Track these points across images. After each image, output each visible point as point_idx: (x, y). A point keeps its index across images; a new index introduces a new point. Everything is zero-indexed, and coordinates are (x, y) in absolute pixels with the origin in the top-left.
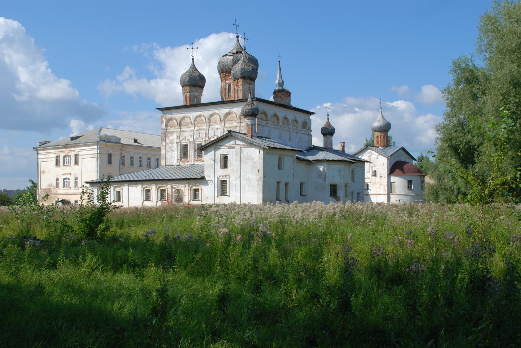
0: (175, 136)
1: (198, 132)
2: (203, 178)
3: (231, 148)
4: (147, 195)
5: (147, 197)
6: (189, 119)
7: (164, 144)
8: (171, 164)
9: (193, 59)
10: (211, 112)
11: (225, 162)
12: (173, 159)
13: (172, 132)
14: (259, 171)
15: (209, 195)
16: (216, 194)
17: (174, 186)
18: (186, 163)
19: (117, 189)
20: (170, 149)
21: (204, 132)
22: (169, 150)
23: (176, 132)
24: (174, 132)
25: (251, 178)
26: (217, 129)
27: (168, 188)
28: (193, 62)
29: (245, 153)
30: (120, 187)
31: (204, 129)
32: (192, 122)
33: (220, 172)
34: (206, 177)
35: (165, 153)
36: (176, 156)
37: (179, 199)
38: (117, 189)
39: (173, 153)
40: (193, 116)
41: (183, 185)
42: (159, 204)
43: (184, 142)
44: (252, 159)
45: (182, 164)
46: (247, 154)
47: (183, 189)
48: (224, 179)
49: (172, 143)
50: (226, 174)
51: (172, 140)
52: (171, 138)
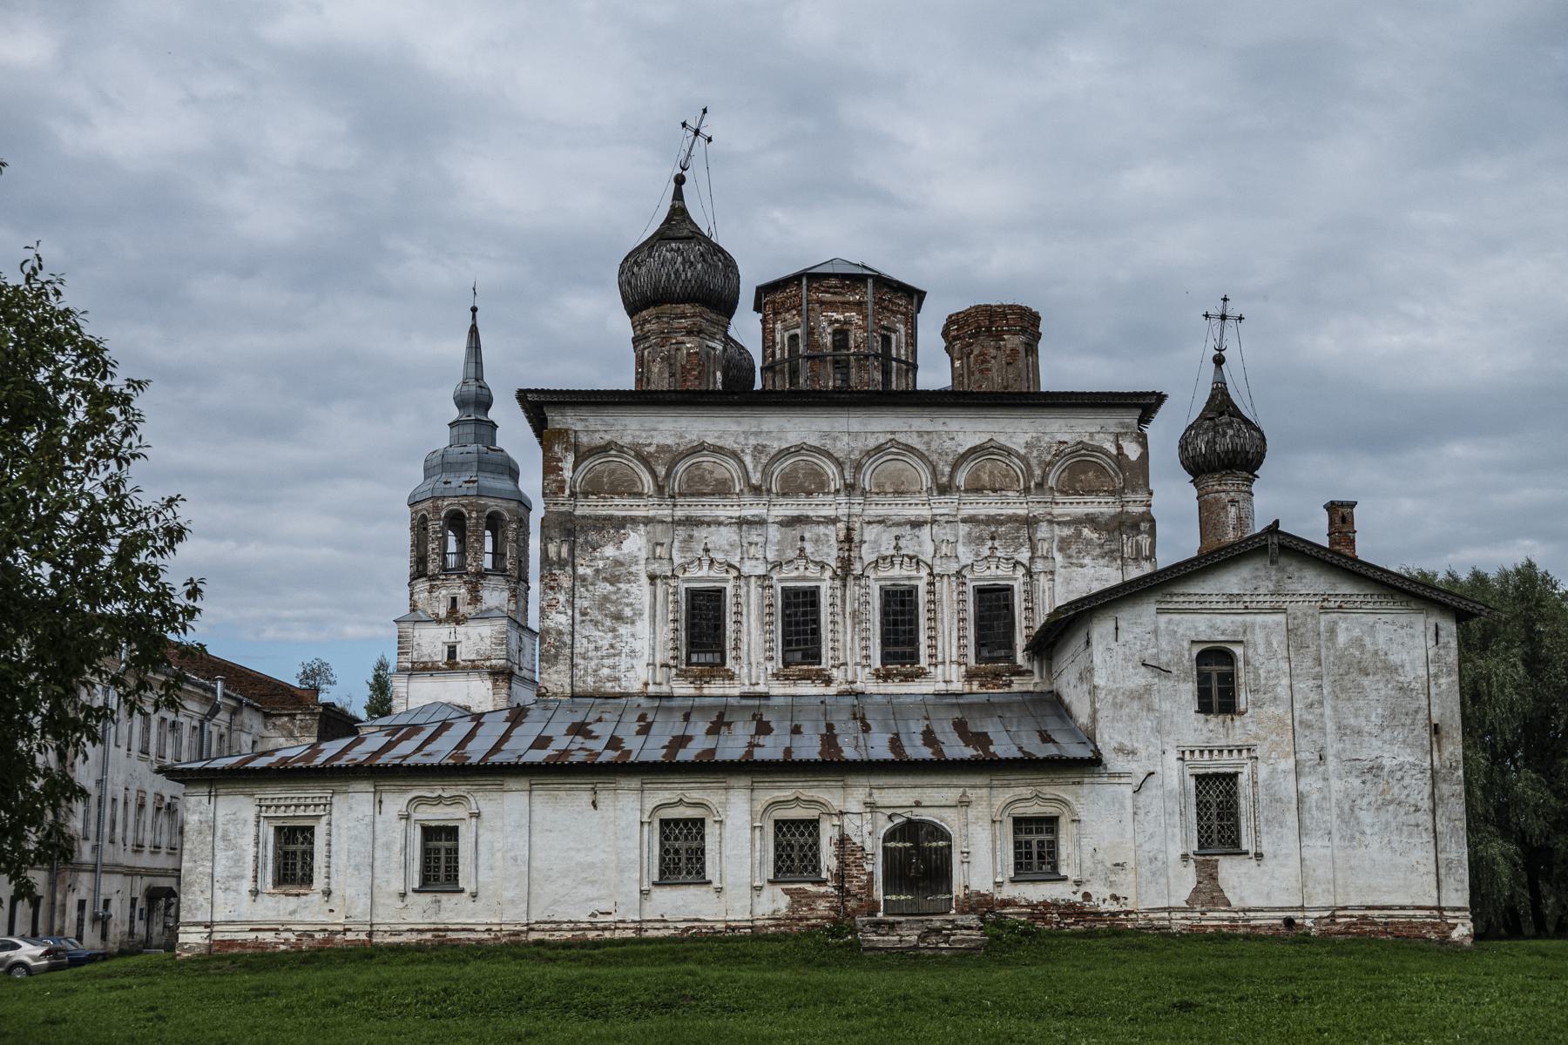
0: (635, 543)
1: (796, 532)
2: (1093, 764)
3: (1260, 611)
4: (681, 852)
6: (732, 464)
7: (566, 582)
9: (680, 180)
11: (1217, 681)
12: (624, 662)
13: (621, 523)
14: (1436, 730)
15: (1127, 852)
16: (1176, 850)
17: (882, 797)
18: (715, 688)
19: (436, 815)
20: (601, 607)
21: (833, 533)
22: (595, 614)
23: (648, 521)
24: (634, 521)
25: (1388, 763)
26: (916, 524)
28: (678, 195)
29: (1342, 639)
30: (456, 800)
31: (833, 521)
32: (756, 479)
33: (1195, 728)
34: (1107, 755)
35: (567, 629)
36: (642, 646)
39: (623, 630)
42: (775, 902)
43: (702, 576)
44: (1392, 669)
45: (683, 688)
47: (950, 820)
48: (1223, 764)
49: (613, 580)
50: (1237, 738)
51: (618, 563)
52: (609, 551)
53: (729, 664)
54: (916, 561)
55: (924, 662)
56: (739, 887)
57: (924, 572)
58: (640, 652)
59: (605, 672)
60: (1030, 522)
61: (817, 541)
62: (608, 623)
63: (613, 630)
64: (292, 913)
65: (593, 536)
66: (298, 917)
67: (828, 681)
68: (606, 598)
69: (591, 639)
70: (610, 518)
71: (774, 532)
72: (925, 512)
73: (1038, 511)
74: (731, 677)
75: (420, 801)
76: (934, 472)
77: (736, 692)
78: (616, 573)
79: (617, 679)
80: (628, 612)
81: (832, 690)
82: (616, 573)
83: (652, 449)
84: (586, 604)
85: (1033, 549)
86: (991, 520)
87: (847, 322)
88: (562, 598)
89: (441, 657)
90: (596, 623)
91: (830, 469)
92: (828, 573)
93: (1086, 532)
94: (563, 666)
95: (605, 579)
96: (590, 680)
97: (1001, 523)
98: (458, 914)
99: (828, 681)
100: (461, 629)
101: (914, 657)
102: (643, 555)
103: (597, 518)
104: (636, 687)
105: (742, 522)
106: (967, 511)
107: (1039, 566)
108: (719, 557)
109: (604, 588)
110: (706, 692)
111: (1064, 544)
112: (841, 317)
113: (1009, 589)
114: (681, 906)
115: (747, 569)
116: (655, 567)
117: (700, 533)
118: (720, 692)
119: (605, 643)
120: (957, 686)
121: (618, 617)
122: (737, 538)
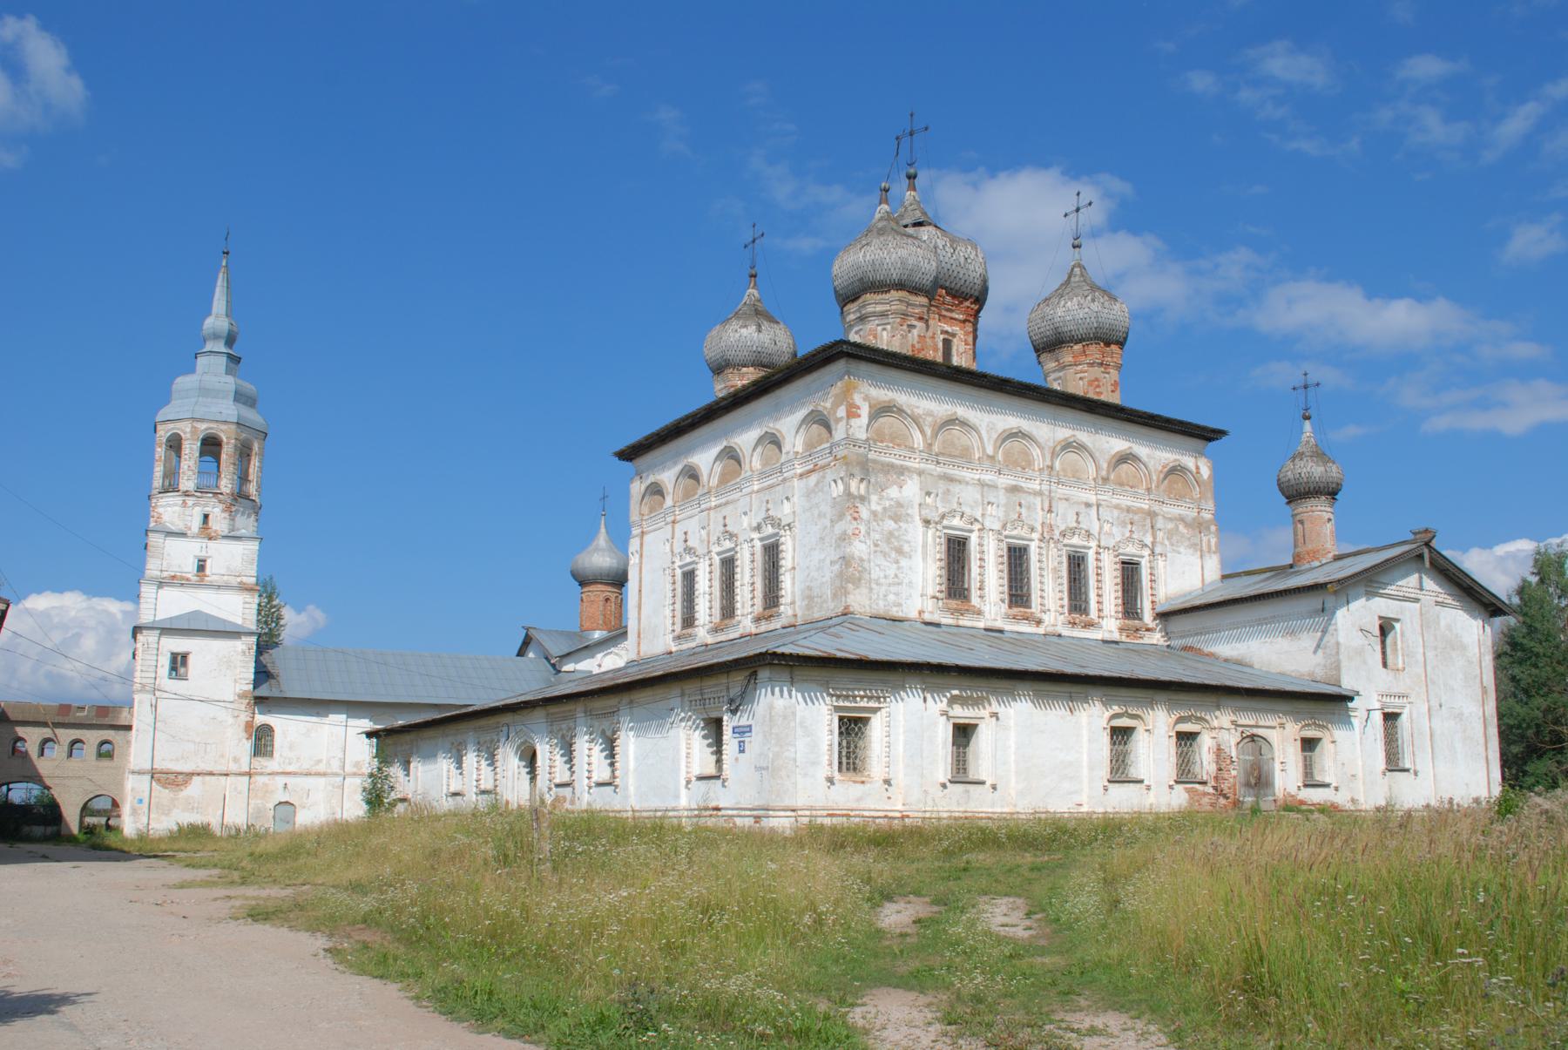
0: (911, 490)
1: (1016, 498)
5: (1120, 772)
8: (895, 612)
10: (1063, 433)
13: (902, 471)
18: (965, 621)
19: (962, 713)
20: (888, 541)
22: (884, 546)
23: (920, 473)
26: (1088, 505)
27: (1221, 730)
30: (977, 702)
31: (1040, 493)
37: (1259, 780)
38: (962, 713)
39: (904, 562)
40: (991, 428)
41: (1271, 720)
42: (1178, 799)
46: (1449, 627)
49: (896, 518)
51: (899, 505)
52: (893, 492)
53: (975, 600)
54: (1089, 534)
55: (1093, 614)
56: (1155, 784)
57: (1093, 544)
58: (913, 586)
59: (891, 597)
60: (1152, 515)
61: (1029, 508)
62: (893, 554)
63: (897, 562)
64: (859, 800)
65: (881, 478)
66: (862, 806)
67: (1039, 622)
68: (891, 533)
69: (880, 569)
70: (892, 466)
71: (1002, 497)
72: (1092, 499)
73: (1156, 507)
74: (979, 613)
75: (953, 701)
76: (1098, 468)
77: (981, 625)
78: (897, 513)
79: (900, 605)
80: (906, 548)
81: (1041, 630)
82: (897, 513)
83: (920, 412)
84: (877, 536)
85: (1154, 537)
86: (1129, 510)
87: (954, 335)
88: (863, 528)
89: (190, 568)
90: (885, 555)
91: (1036, 452)
92: (1035, 536)
93: (1181, 528)
94: (864, 591)
95: (891, 518)
96: (881, 603)
97: (1135, 513)
98: (982, 804)
99: (1039, 622)
100: (211, 544)
101: (1085, 611)
102: (917, 500)
103: (883, 464)
104: (913, 614)
105: (982, 484)
106: (1115, 501)
107: (1158, 550)
108: (968, 511)
109: (890, 525)
110: (961, 623)
111: (1170, 534)
112: (949, 329)
113: (1138, 564)
114: (1122, 800)
115: (987, 524)
116: (927, 513)
117: (955, 488)
118: (969, 624)
119: (891, 572)
120: (1116, 636)
121: (900, 551)
122: (979, 497)
